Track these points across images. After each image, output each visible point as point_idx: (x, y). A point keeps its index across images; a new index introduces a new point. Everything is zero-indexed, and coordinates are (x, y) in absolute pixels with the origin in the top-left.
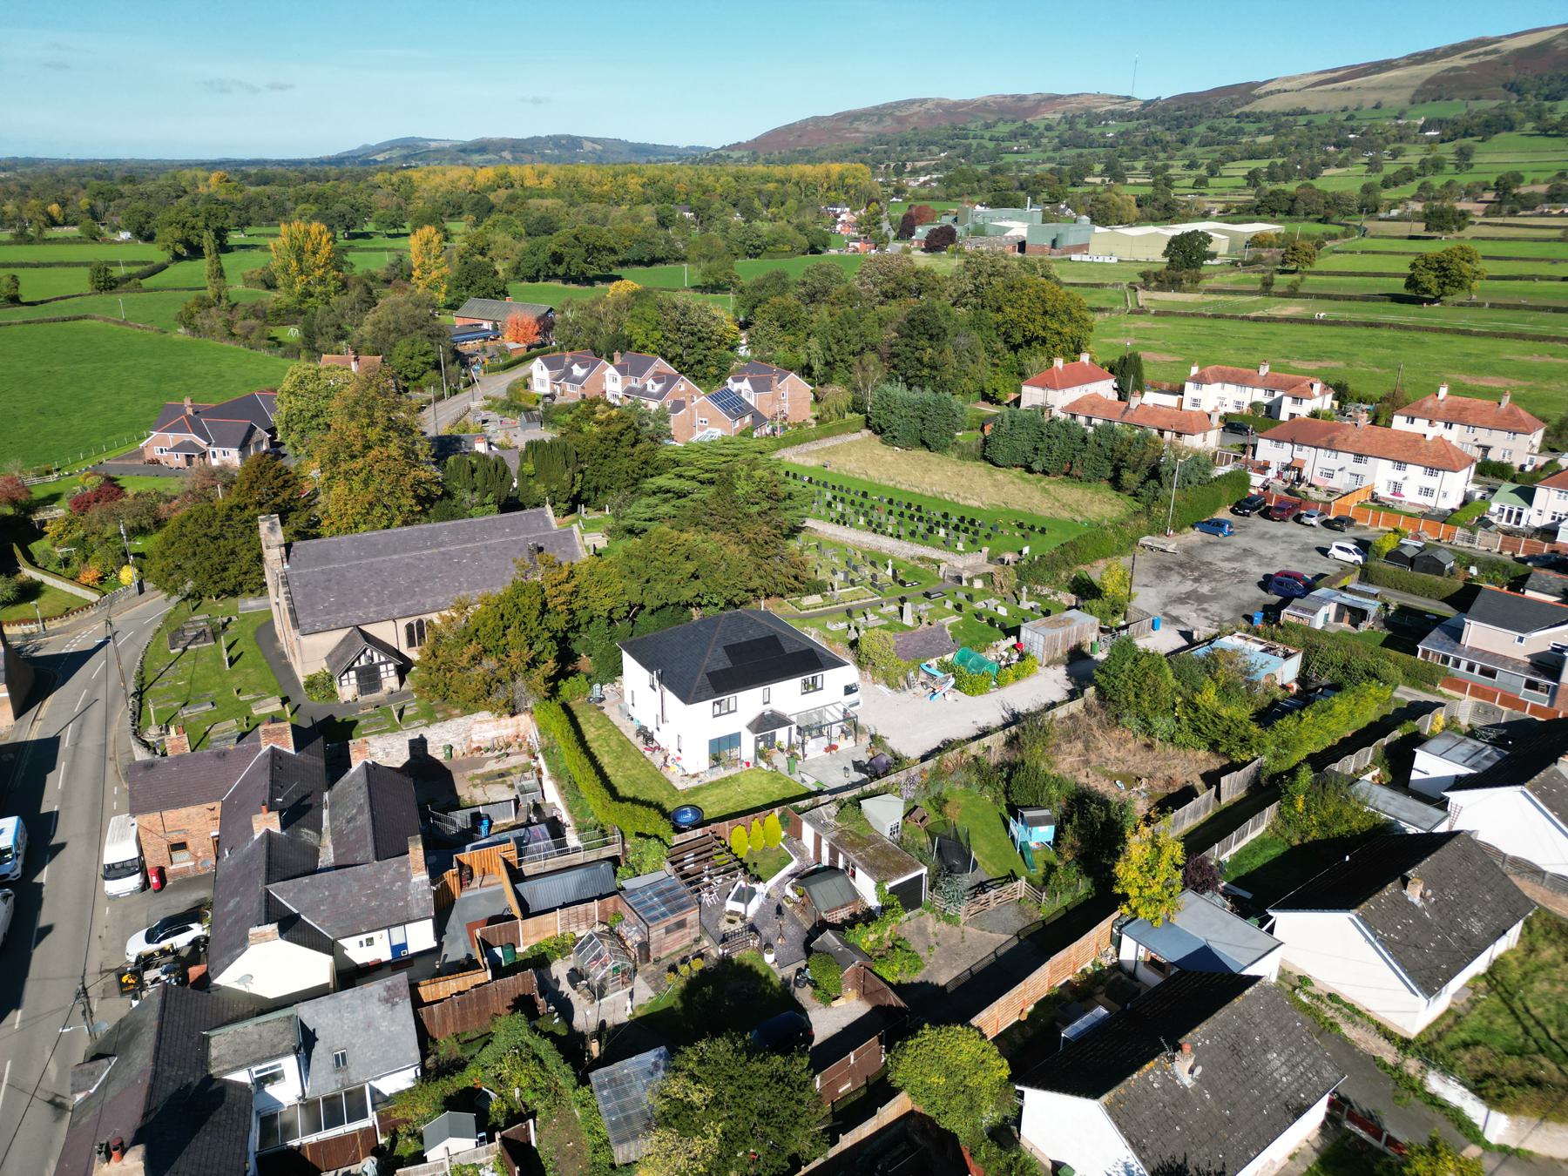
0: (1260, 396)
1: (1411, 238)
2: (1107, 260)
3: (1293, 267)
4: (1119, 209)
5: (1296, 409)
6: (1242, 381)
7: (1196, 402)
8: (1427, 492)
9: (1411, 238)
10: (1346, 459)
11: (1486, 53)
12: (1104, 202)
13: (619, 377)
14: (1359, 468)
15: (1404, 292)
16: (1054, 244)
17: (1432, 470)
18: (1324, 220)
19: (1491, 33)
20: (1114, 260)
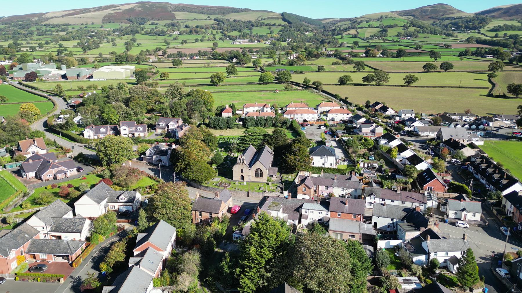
0: (258, 108)
1: (170, 68)
2: (103, 80)
3: (163, 78)
4: (72, 62)
5: (267, 110)
6: (253, 106)
8: (313, 118)
9: (170, 68)
10: (299, 115)
11: (118, 9)
12: (66, 60)
13: (127, 128)
14: (302, 116)
15: (210, 83)
16: (78, 76)
17: (313, 114)
18: (138, 63)
19: (116, 3)
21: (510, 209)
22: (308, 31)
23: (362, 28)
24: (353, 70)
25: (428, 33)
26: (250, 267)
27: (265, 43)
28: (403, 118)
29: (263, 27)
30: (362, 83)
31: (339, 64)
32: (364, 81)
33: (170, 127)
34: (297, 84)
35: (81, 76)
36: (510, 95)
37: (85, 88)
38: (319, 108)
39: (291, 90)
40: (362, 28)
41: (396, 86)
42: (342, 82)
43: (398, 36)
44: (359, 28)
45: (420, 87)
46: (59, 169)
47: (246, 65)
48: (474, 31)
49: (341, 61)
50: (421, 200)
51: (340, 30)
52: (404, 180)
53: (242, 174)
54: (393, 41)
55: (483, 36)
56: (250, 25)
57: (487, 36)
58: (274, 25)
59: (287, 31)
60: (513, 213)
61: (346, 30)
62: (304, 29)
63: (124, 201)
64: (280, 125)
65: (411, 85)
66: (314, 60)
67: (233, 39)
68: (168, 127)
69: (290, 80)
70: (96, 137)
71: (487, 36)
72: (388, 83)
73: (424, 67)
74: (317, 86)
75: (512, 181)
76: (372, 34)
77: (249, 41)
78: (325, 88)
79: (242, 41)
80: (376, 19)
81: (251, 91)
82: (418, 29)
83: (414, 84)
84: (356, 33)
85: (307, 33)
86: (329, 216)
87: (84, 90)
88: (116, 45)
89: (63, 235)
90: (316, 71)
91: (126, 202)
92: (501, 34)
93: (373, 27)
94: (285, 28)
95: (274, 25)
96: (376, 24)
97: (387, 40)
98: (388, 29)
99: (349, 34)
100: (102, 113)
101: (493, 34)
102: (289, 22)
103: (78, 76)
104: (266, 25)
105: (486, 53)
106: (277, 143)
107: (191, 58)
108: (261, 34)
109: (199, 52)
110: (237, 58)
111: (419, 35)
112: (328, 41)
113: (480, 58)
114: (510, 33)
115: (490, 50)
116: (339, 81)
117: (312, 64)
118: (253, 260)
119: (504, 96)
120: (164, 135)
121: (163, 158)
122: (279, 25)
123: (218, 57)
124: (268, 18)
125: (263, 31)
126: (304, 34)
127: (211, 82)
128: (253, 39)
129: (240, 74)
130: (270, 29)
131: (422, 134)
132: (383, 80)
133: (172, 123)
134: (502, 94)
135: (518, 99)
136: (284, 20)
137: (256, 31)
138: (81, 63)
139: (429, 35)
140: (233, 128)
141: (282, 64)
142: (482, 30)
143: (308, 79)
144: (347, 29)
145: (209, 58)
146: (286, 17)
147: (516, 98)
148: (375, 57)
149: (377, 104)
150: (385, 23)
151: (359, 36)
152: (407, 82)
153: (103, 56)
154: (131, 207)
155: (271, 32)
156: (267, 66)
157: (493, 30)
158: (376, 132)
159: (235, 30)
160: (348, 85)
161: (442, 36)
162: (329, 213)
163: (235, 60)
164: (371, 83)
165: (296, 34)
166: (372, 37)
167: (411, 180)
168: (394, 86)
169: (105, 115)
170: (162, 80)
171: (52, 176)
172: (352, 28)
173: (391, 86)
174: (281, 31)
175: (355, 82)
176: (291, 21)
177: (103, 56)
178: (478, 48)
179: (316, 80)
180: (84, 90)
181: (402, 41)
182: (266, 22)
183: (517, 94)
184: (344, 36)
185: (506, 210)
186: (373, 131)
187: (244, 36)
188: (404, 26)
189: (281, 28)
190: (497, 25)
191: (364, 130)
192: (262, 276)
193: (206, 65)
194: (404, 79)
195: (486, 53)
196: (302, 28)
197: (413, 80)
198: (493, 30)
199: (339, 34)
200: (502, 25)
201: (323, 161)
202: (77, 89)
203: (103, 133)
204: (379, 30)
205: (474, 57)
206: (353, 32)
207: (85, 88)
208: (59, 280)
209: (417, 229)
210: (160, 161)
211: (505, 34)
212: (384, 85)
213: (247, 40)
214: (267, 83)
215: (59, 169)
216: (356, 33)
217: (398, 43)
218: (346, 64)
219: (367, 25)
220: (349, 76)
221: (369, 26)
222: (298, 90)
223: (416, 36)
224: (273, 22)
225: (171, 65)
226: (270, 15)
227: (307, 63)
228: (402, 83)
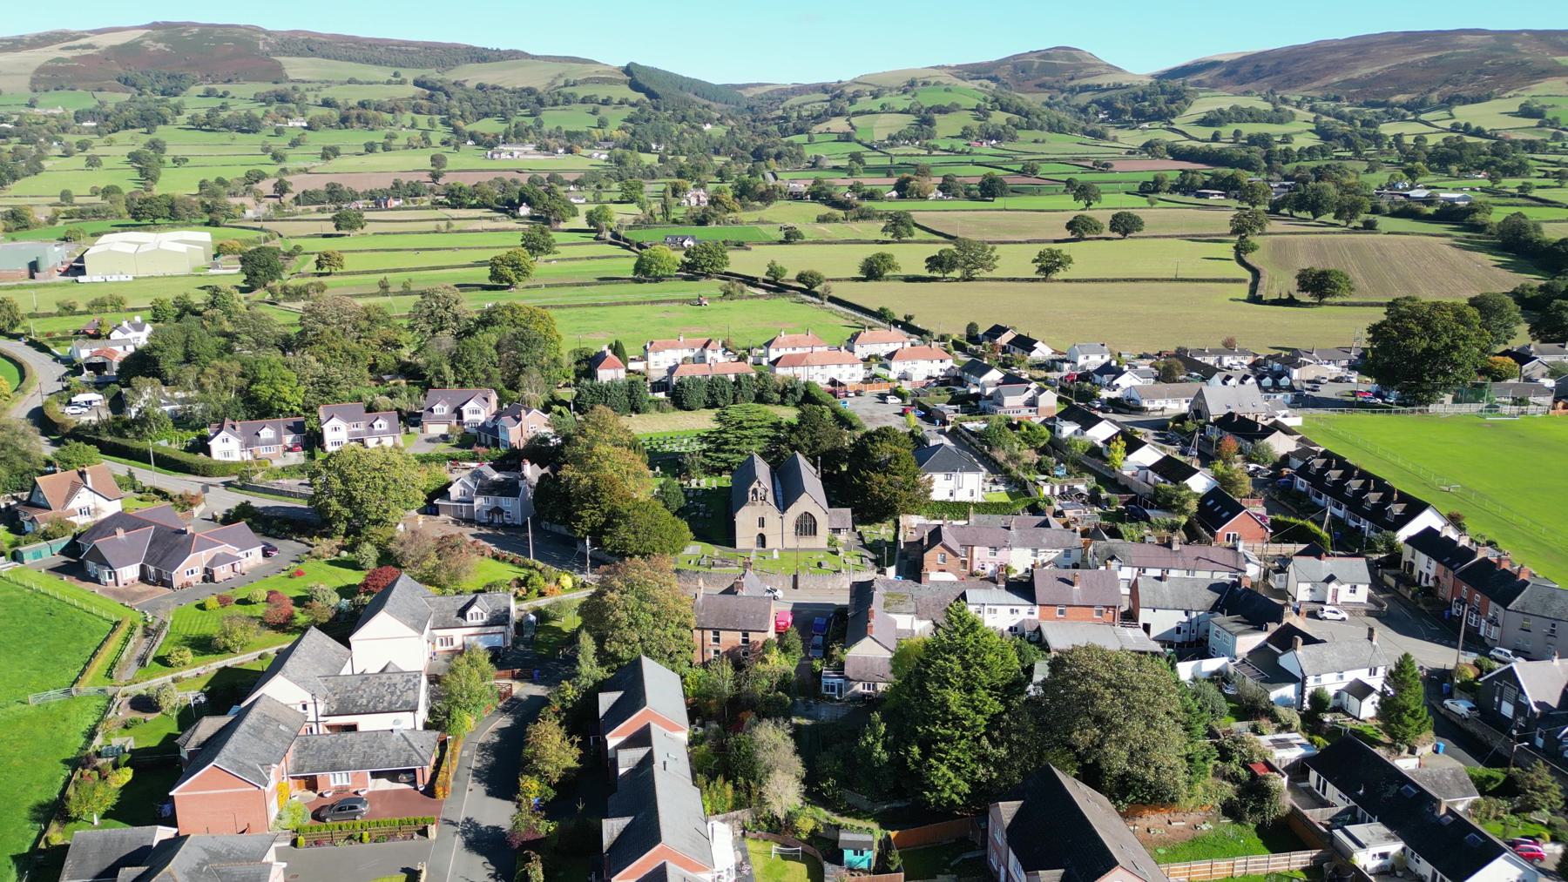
2: (123, 278)
3: (326, 270)
6: (673, 347)
7: (656, 363)
10: (817, 368)
13: (343, 425)
15: (488, 283)
16: (34, 267)
19: (74, 26)
20: (130, 278)
21: (1425, 571)
22: (709, 121)
23: (862, 113)
24: (882, 237)
25: (1041, 129)
26: (948, 740)
27: (590, 157)
28: (1083, 367)
29: (572, 106)
30: (926, 273)
31: (836, 220)
32: (931, 269)
33: (467, 417)
34: (751, 281)
35: (42, 267)
36: (1305, 297)
37: (81, 307)
38: (857, 348)
39: (740, 298)
40: (862, 113)
41: (1014, 280)
42: (872, 271)
43: (963, 136)
44: (856, 114)
45: (1077, 281)
46: (218, 550)
47: (562, 226)
48: (1156, 124)
49: (840, 213)
50: (1232, 562)
51: (799, 117)
52: (1169, 520)
53: (760, 530)
54: (952, 150)
55: (1182, 137)
56: (534, 101)
57: (1191, 138)
58: (606, 102)
59: (648, 121)
60: (1436, 578)
61: (818, 118)
62: (698, 116)
63: (480, 621)
64: (777, 397)
65: (1054, 277)
66: (759, 209)
67: (486, 143)
68: (460, 416)
69: (726, 269)
70: (248, 457)
71: (1191, 138)
72: (996, 274)
73: (1070, 226)
74: (811, 286)
75: (1415, 507)
76: (894, 132)
77: (539, 149)
78: (838, 291)
79: (517, 150)
80: (899, 89)
81: (626, 303)
82: (1016, 118)
83: (1061, 274)
84: (848, 129)
85: (708, 127)
86: (1036, 616)
87: (81, 313)
88: (99, 164)
89: (366, 723)
90: (781, 242)
91: (486, 625)
92: (1227, 131)
93: (893, 111)
94: (642, 111)
95: (606, 102)
96: (901, 102)
97: (935, 148)
98: (936, 116)
99: (828, 132)
100: (252, 383)
101: (1208, 132)
102: (651, 94)
103: (34, 267)
104: (584, 101)
105: (1206, 185)
106: (816, 444)
107: (378, 204)
108: (573, 129)
109: (396, 185)
110: (529, 205)
111: (1020, 133)
112: (774, 151)
113: (1191, 199)
114: (1249, 129)
115: (1214, 176)
116: (863, 269)
117: (761, 222)
118: (957, 721)
119: (1291, 302)
120: (456, 441)
121: (506, 503)
122: (621, 103)
123: (467, 201)
124: (586, 81)
125: (576, 119)
126: (700, 130)
127: (491, 278)
128: (552, 143)
129: (565, 252)
130: (594, 112)
131: (1150, 407)
132: (982, 266)
133: (471, 405)
134: (1285, 296)
135: (1325, 308)
136: (635, 86)
137: (552, 119)
138: (11, 224)
139: (1045, 135)
140: (645, 411)
141: (675, 222)
142: (1178, 123)
143: (778, 264)
144: (819, 116)
145: (437, 205)
146: (640, 79)
147: (1320, 304)
148: (926, 198)
149: (997, 331)
150: (927, 99)
151: (858, 137)
152: (1042, 269)
153: (77, 200)
154: (499, 637)
155: (602, 124)
156: (630, 227)
157: (1205, 122)
158: (1041, 404)
159: (486, 115)
160: (888, 279)
161: (1078, 137)
162: (1037, 609)
163: (524, 210)
164: (951, 275)
165: (675, 129)
166: (893, 140)
167: (1184, 520)
168: (1009, 280)
169: (263, 391)
170: (320, 275)
171: (199, 574)
172: (837, 115)
173: (1002, 280)
174: (630, 120)
175: (905, 272)
176: (657, 90)
177: (77, 200)
178: (1185, 172)
179: (805, 269)
180: (81, 313)
181: (976, 150)
182: (581, 92)
183: (1322, 295)
184: (817, 138)
185: (1416, 573)
186: (1032, 403)
187: (519, 135)
188: (978, 109)
189: (627, 111)
190: (1215, 108)
191: (1009, 401)
192: (983, 759)
193: (443, 224)
194: (1035, 261)
195: (1206, 185)
196: (691, 113)
197: (1060, 264)
198: (1205, 122)
199: (800, 132)
200: (1226, 108)
201: (951, 484)
202: (55, 310)
203: (269, 442)
204: (911, 119)
205: (1177, 197)
206: (839, 124)
207: (81, 307)
208: (424, 832)
209: (1260, 627)
210: (498, 510)
211: (1237, 133)
212: (983, 280)
213: (530, 148)
214: (658, 279)
215: (218, 550)
216: (848, 129)
217: (969, 158)
218: (856, 219)
219: (875, 105)
220: (891, 256)
221: (883, 107)
222: (758, 296)
223: (1013, 138)
224: (602, 92)
225: (330, 228)
226: (591, 71)
227: (745, 216)
228: (1031, 271)
